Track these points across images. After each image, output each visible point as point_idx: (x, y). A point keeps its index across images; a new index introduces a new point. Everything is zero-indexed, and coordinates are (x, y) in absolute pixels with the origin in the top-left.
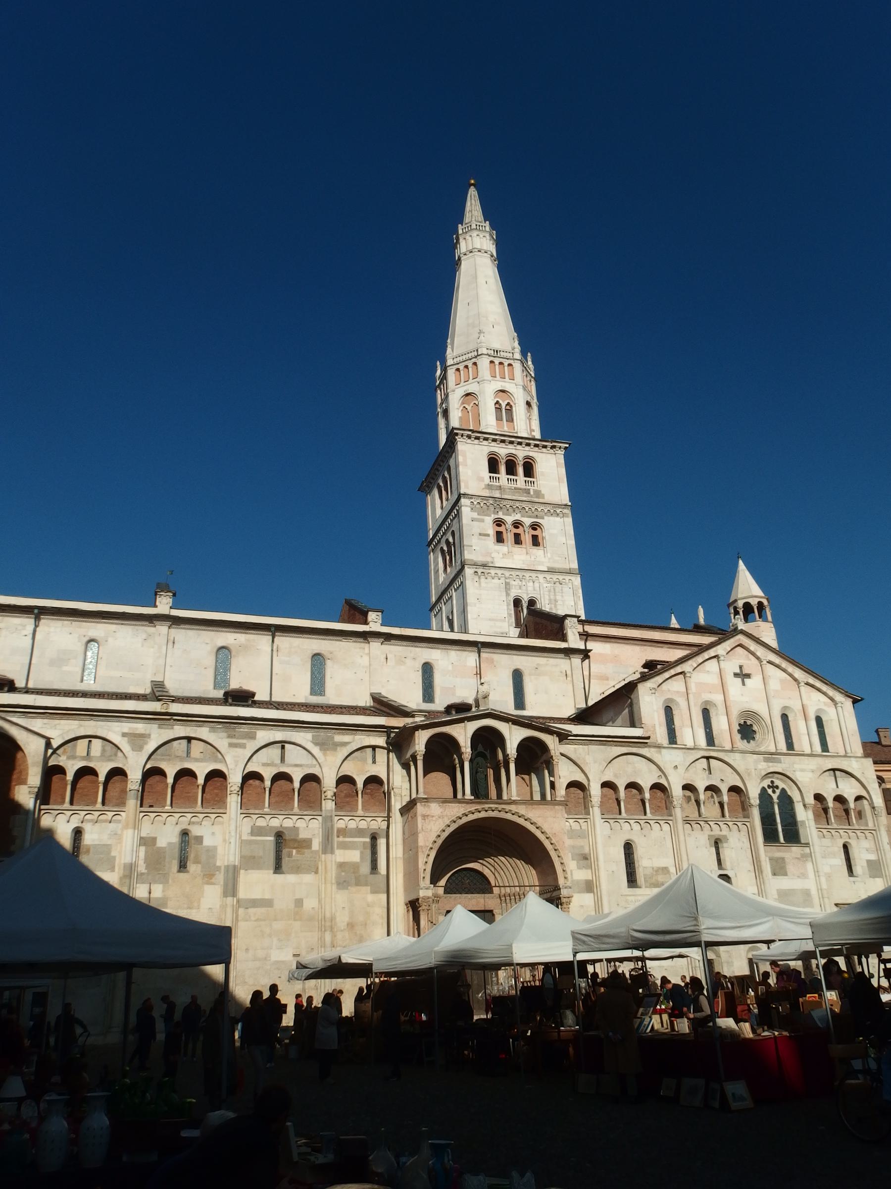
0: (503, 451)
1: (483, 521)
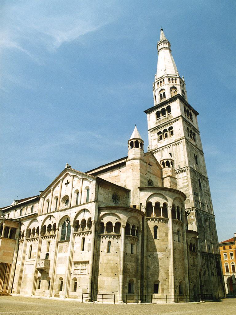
0: (160, 110)
1: (154, 135)
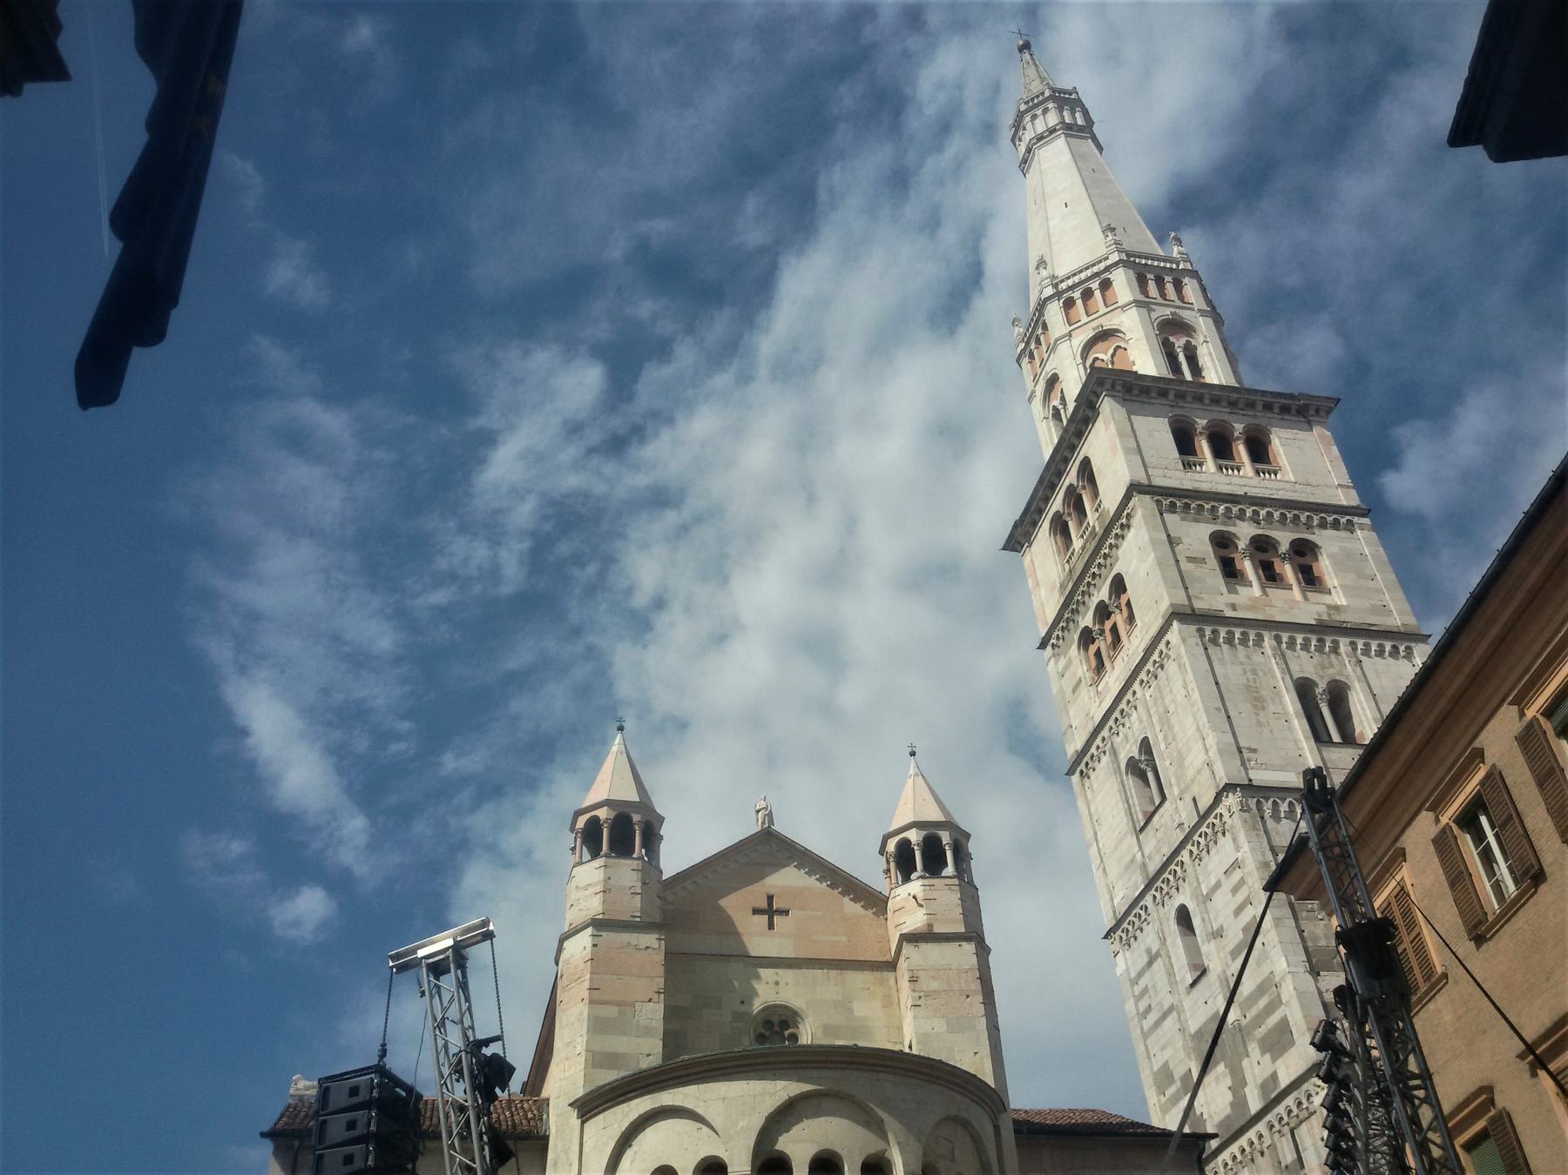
1: (1069, 663)
